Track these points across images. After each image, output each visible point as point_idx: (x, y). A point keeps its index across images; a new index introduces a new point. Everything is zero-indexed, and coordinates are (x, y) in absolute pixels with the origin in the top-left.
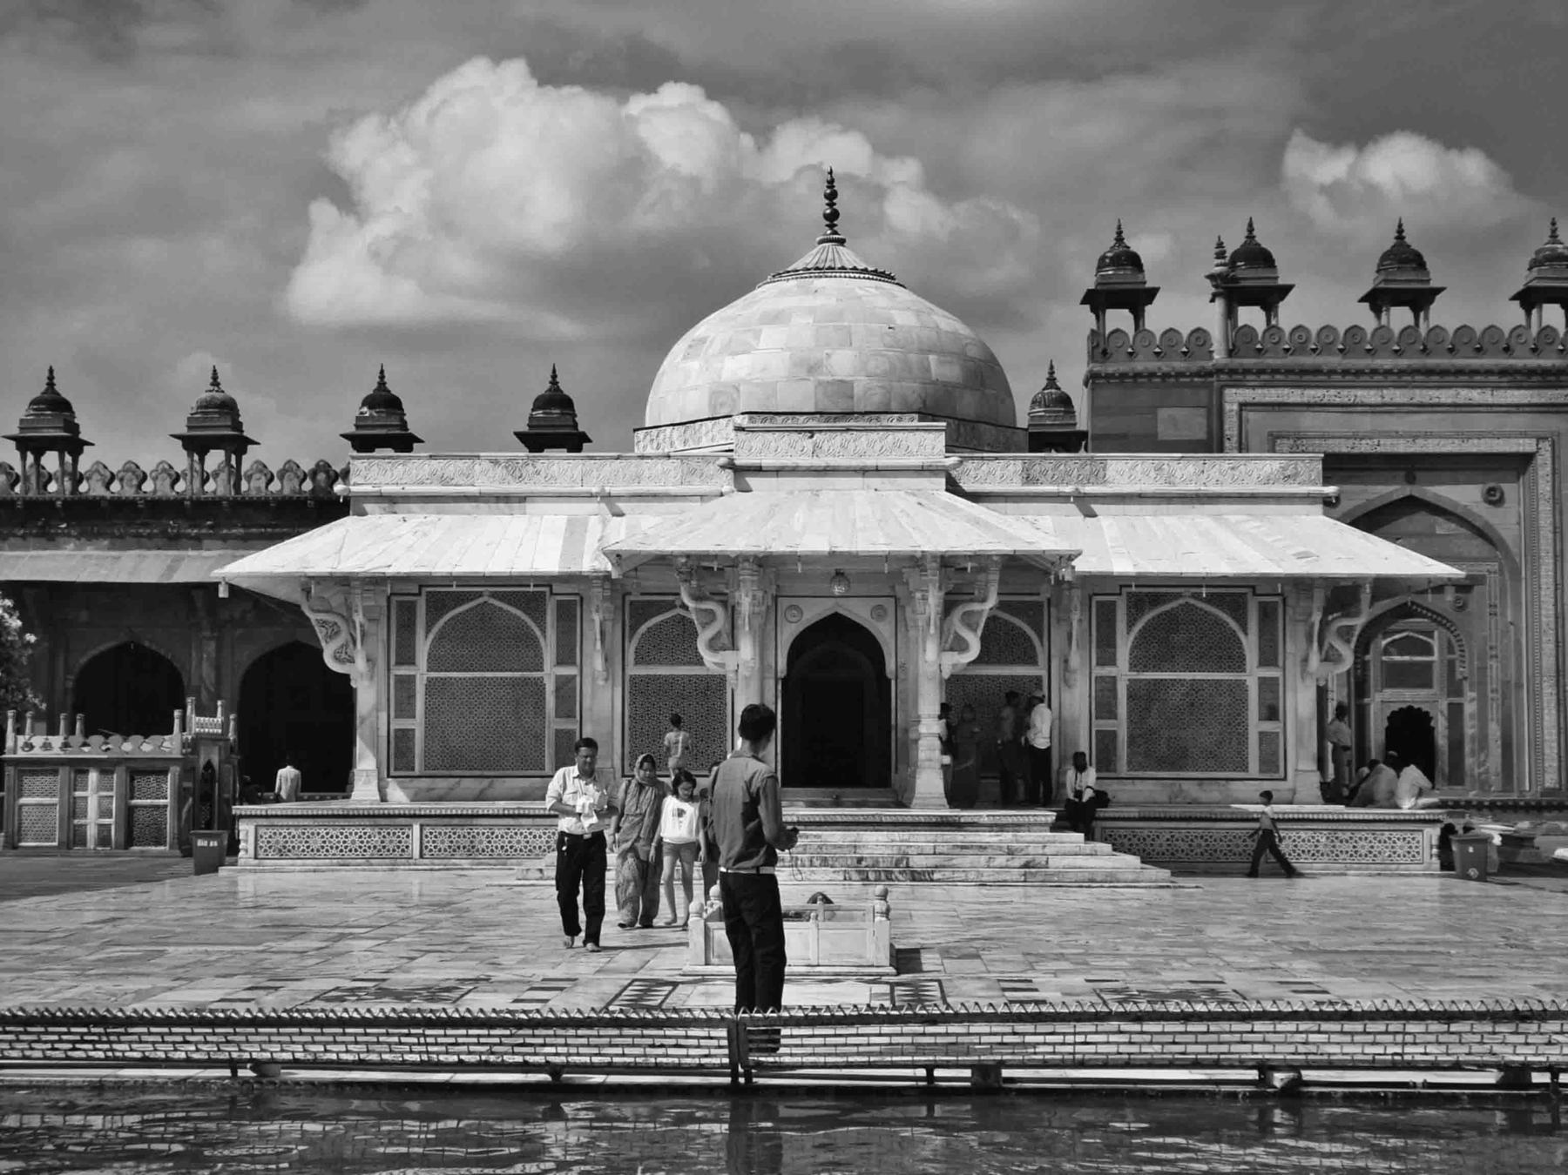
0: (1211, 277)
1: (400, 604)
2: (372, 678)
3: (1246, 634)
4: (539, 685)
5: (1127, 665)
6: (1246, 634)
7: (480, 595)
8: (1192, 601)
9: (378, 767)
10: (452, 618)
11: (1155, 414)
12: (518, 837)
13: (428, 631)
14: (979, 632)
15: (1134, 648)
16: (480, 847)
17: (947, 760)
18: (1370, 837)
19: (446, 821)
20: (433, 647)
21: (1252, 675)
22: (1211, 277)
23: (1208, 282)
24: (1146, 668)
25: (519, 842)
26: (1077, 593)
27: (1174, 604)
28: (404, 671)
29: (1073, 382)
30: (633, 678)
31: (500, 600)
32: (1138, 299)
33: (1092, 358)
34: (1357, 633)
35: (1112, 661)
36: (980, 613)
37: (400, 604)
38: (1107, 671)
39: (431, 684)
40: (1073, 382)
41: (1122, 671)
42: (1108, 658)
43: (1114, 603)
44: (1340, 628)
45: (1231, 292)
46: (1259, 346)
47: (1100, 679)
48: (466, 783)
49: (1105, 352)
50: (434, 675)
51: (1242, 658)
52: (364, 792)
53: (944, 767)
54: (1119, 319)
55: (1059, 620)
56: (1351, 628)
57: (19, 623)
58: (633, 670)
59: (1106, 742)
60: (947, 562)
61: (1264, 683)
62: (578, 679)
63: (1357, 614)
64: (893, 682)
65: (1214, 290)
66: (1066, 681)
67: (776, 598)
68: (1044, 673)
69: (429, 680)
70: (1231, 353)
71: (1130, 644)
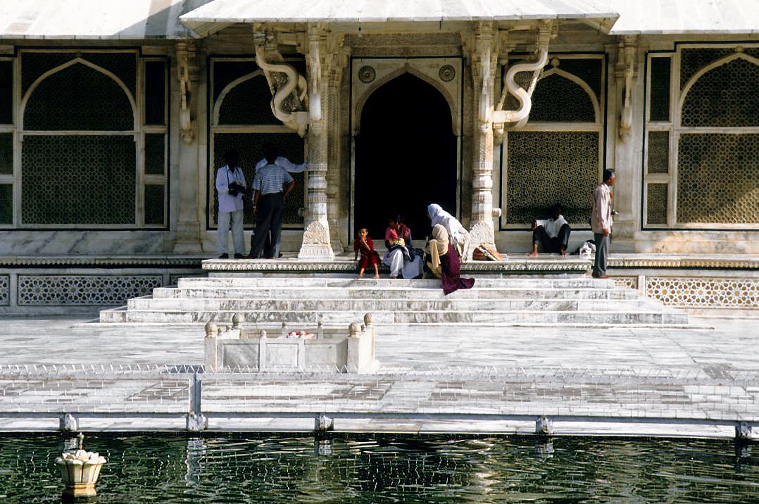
4: (130, 141)
5: (680, 121)
7: (73, 56)
8: (744, 57)
10: (47, 79)
12: (108, 286)
15: (687, 103)
16: (73, 294)
19: (41, 271)
24: (696, 123)
25: (108, 291)
26: (631, 51)
27: (727, 60)
30: (217, 136)
36: (531, 74)
39: (27, 141)
41: (675, 127)
42: (660, 110)
43: (668, 60)
55: (615, 78)
58: (218, 129)
60: (500, 26)
62: (166, 136)
64: (459, 139)
66: (620, 137)
67: (351, 59)
69: (26, 138)
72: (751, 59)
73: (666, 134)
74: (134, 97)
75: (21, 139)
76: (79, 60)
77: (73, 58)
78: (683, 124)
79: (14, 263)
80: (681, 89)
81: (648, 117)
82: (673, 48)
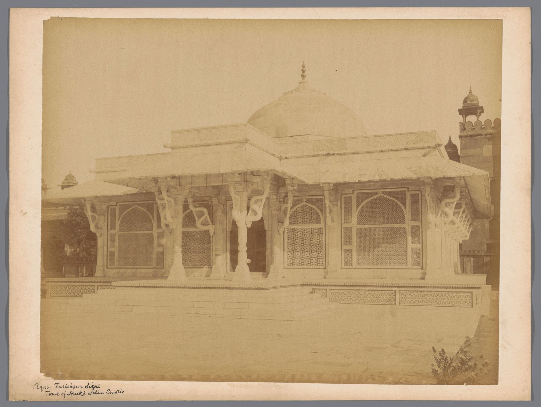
1: (111, 208)
3: (405, 208)
5: (356, 224)
6: (405, 208)
7: (134, 205)
8: (382, 195)
9: (104, 265)
15: (359, 215)
17: (249, 261)
18: (447, 294)
21: (408, 224)
24: (364, 224)
27: (376, 197)
28: (113, 231)
29: (457, 142)
31: (140, 206)
33: (460, 132)
37: (111, 208)
38: (349, 225)
48: (129, 270)
53: (248, 264)
54: (472, 119)
57: (73, 223)
61: (413, 227)
63: (454, 197)
64: (267, 232)
68: (323, 227)
71: (357, 214)
72: (386, 196)
74: (153, 219)
75: (118, 235)
76: (136, 206)
77: (135, 205)
78: (358, 224)
79: (95, 281)
80: (356, 209)
81: (343, 221)
82: (352, 192)
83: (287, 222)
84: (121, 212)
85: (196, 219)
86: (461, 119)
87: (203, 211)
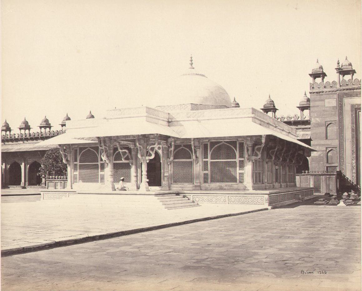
0: (336, 69)
2: (69, 165)
3: (236, 150)
6: (236, 150)
8: (224, 143)
11: (323, 100)
13: (79, 154)
14: (154, 152)
17: (148, 180)
20: (80, 158)
21: (237, 160)
22: (336, 69)
23: (336, 70)
27: (221, 144)
28: (75, 163)
32: (324, 75)
34: (262, 149)
35: (207, 158)
40: (309, 96)
41: (209, 160)
43: (207, 144)
44: (257, 148)
45: (342, 72)
46: (347, 84)
47: (205, 162)
49: (313, 88)
50: (81, 164)
51: (235, 156)
52: (68, 188)
54: (318, 80)
56: (261, 148)
59: (206, 176)
61: (240, 161)
65: (337, 72)
70: (341, 86)
72: (226, 144)
73: (207, 162)
83: (172, 158)
84: (80, 152)
85: (122, 156)
86: (311, 79)
87: (126, 152)
